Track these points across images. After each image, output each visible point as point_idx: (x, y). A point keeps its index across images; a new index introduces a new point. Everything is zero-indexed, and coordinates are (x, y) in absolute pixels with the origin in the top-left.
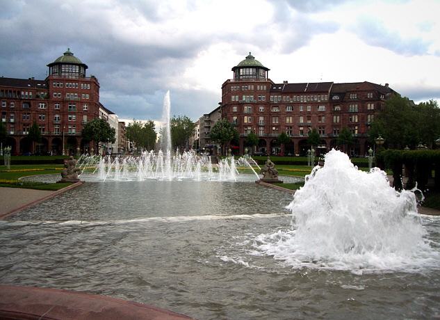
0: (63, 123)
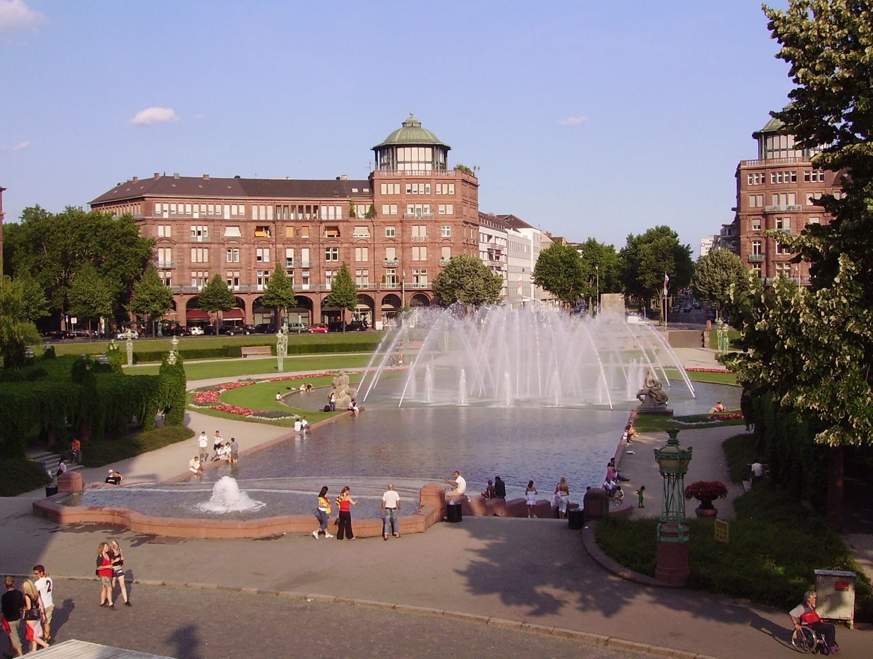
0: (403, 264)
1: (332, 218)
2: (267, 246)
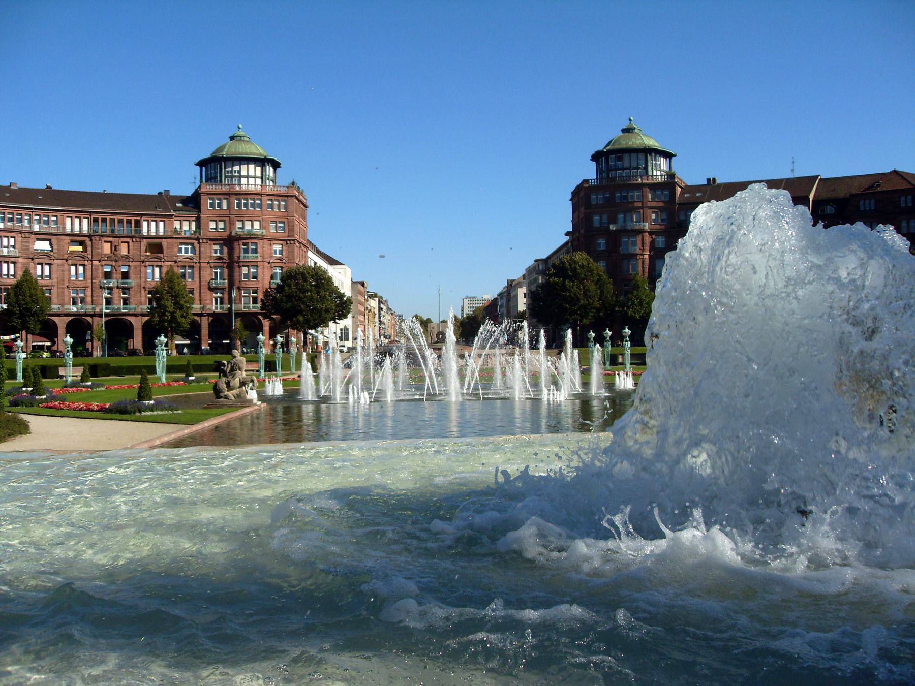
1: (153, 233)
2: (82, 262)
